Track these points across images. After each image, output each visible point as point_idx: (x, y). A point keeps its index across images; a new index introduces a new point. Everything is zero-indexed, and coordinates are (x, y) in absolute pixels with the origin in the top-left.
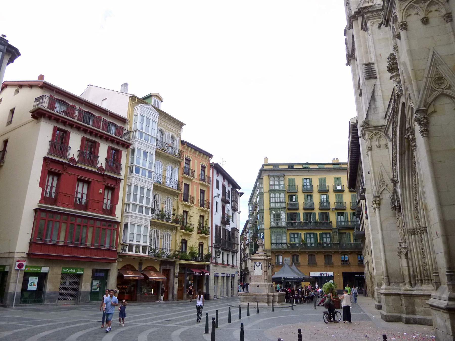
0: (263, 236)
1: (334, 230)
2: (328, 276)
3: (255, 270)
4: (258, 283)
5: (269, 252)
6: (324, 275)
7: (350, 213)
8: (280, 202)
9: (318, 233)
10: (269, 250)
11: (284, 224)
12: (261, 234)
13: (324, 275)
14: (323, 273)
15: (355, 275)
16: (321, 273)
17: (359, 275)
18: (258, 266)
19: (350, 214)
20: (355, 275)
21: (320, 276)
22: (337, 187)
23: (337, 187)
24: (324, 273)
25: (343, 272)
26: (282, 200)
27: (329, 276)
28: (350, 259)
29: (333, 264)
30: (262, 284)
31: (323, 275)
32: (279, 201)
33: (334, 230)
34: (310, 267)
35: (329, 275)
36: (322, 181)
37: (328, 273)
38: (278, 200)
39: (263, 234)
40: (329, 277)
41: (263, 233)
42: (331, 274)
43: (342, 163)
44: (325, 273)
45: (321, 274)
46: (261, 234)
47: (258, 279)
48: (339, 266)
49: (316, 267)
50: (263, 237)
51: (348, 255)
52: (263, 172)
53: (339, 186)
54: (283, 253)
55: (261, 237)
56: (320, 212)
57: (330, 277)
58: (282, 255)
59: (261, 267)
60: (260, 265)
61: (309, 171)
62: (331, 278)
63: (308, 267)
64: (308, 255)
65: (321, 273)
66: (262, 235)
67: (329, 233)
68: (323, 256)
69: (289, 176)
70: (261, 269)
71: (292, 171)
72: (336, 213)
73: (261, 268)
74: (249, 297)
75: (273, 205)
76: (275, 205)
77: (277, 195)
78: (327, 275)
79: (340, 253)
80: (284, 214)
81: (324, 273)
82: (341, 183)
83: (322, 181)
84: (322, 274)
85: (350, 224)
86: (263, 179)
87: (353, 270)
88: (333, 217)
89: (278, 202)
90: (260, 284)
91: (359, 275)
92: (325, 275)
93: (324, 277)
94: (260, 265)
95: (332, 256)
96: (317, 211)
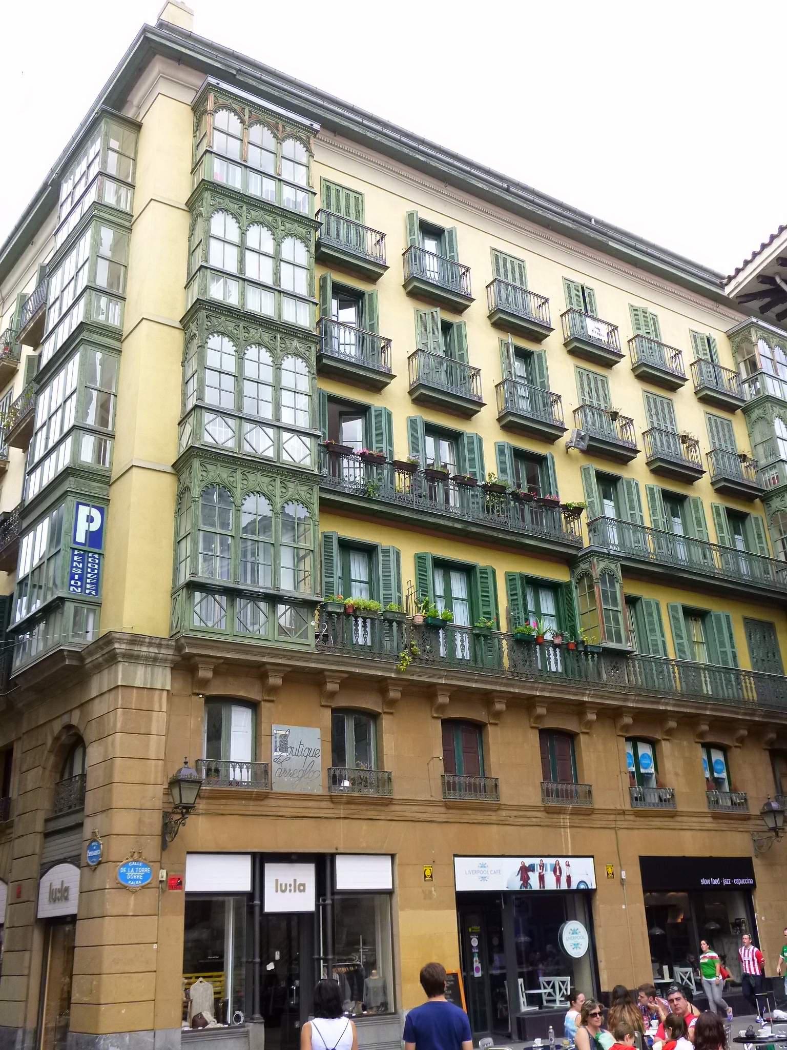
0: (95, 526)
1: (602, 565)
2: (564, 886)
5: (154, 661)
6: (542, 878)
10: (153, 642)
12: (84, 511)
13: (542, 878)
14: (536, 861)
15: (704, 882)
16: (528, 862)
19: (652, 498)
20: (704, 882)
21: (516, 885)
24: (542, 866)
25: (643, 854)
27: (574, 886)
28: (669, 765)
31: (535, 884)
33: (602, 565)
34: (453, 815)
35: (569, 879)
37: (562, 861)
39: (96, 514)
40: (570, 892)
41: (102, 504)
44: (550, 862)
45: (525, 871)
46: (84, 511)
48: (623, 813)
49: (493, 817)
50: (96, 538)
52: (158, 66)
54: (275, 680)
55: (81, 537)
57: (578, 891)
58: (253, 705)
63: (440, 813)
65: (528, 862)
66: (90, 519)
67: (553, 587)
75: (217, 291)
76: (243, 295)
77: (259, 237)
78: (558, 880)
79: (628, 720)
84: (531, 868)
86: (137, 126)
91: (716, 882)
92: (551, 884)
93: (544, 895)
95: (583, 738)
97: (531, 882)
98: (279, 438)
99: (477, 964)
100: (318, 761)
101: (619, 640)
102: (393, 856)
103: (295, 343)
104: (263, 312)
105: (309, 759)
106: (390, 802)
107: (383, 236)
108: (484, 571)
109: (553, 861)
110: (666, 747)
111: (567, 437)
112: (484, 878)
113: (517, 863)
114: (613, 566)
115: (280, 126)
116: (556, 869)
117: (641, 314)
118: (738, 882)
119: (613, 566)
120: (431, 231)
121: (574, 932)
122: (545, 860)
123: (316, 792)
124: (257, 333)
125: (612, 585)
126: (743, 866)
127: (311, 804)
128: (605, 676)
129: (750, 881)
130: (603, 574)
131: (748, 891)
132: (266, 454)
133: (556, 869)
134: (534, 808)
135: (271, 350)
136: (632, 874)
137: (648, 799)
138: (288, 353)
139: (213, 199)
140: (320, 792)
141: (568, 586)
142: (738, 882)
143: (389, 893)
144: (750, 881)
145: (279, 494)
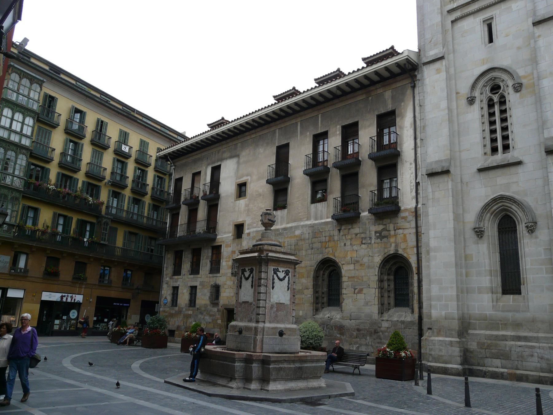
2: (73, 301)
3: (273, 288)
4: (281, 326)
6: (67, 299)
7: (129, 197)
8: (21, 134)
9: (75, 218)
11: (18, 183)
13: (67, 299)
14: (67, 294)
16: (64, 294)
17: (118, 304)
18: (281, 280)
21: (59, 300)
22: (123, 146)
23: (123, 146)
25: (99, 295)
26: (27, 131)
27: (76, 301)
28: (112, 274)
29: (85, 279)
30: (290, 329)
31: (64, 299)
32: (18, 130)
33: (105, 220)
35: (75, 300)
36: (101, 126)
37: (74, 295)
38: (16, 126)
42: (79, 298)
43: (137, 111)
44: (70, 295)
45: (62, 297)
47: (279, 313)
48: (95, 285)
51: (110, 268)
53: (126, 146)
56: (86, 180)
57: (77, 303)
59: (289, 284)
60: (285, 277)
61: (88, 99)
62: (76, 306)
64: (48, 257)
65: (64, 294)
67: (92, 224)
68: (73, 264)
69: (50, 89)
70: (288, 289)
71: (56, 82)
72: (109, 191)
73: (288, 287)
74: (286, 365)
76: (10, 135)
77: (18, 116)
78: (72, 300)
79: (103, 262)
80: (24, 163)
81: (68, 296)
82: (127, 143)
83: (101, 126)
84: (64, 296)
85: (124, 214)
87: (113, 294)
88: (104, 196)
89: (15, 132)
90: (286, 329)
91: (118, 304)
92: (69, 300)
93: (66, 303)
94: (285, 277)
96: (81, 177)
97: (63, 299)
98: (13, 179)
99: (44, 318)
100: (8, 264)
101: (105, 241)
102: (25, 290)
103: (24, 151)
104: (15, 141)
105: (5, 264)
106: (27, 276)
107: (60, 115)
108: (69, 217)
109: (71, 295)
110: (113, 269)
111: (106, 181)
112: (50, 297)
113: (61, 294)
114: (108, 221)
115: (33, 80)
116: (72, 297)
117: (143, 143)
118: (125, 305)
119: (108, 221)
120: (77, 111)
121: (74, 312)
122: (69, 295)
123: (6, 272)
124: (12, 147)
125: (107, 226)
126: (128, 301)
127: (3, 275)
128: (98, 250)
129: (128, 305)
130: (104, 223)
131: (128, 307)
132: (8, 183)
133: (72, 297)
134: (69, 281)
135: (16, 153)
136: (93, 300)
137: (105, 282)
138: (20, 153)
139: (5, 103)
140: (7, 273)
141: (94, 223)
142: (125, 305)
143: (22, 299)
144: (128, 305)
145: (10, 195)
